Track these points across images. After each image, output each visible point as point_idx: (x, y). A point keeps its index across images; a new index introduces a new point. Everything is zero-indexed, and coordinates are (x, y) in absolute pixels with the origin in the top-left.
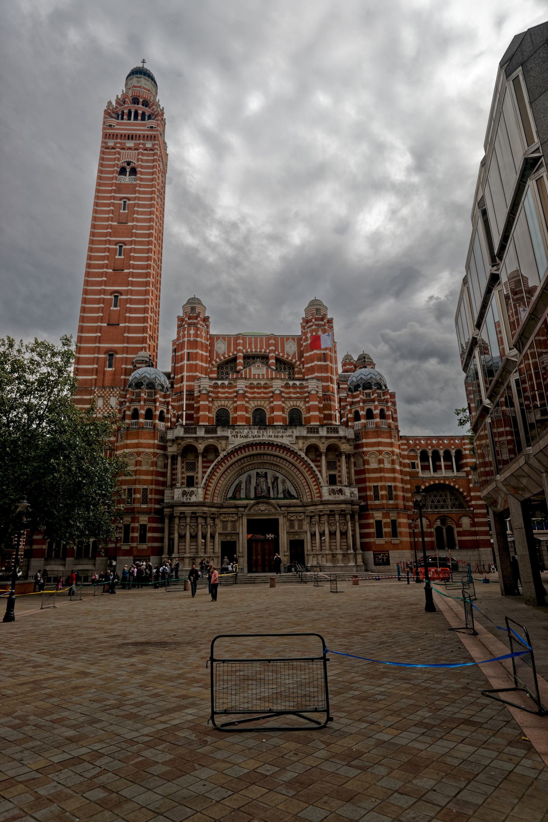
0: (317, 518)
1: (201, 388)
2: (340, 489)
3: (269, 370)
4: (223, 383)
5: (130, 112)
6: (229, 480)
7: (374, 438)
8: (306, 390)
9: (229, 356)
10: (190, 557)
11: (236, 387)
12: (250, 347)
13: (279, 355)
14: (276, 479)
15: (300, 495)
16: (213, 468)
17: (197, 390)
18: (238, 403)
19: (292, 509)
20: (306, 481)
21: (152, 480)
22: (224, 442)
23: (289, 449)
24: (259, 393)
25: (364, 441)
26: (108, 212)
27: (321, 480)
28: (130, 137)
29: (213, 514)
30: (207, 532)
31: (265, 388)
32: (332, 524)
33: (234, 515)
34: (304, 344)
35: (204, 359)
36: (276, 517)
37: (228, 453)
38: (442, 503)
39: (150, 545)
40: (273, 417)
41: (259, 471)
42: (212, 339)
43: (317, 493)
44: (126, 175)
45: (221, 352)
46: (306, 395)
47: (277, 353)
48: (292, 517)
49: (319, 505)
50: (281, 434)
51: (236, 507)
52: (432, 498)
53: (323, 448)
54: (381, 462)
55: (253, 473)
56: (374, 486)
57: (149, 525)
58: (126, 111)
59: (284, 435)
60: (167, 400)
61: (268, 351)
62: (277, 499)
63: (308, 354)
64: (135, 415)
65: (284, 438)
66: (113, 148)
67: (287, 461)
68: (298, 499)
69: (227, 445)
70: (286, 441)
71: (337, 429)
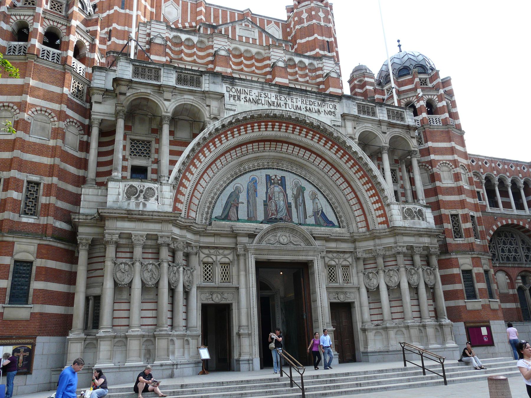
0: (380, 261)
1: (152, 37)
2: (420, 211)
3: (264, 35)
4: (188, 40)
6: (216, 184)
7: (444, 141)
8: (320, 72)
10: (143, 336)
11: (212, 47)
14: (301, 190)
15: (342, 222)
16: (193, 150)
17: (144, 40)
19: (332, 245)
21: (52, 167)
22: (214, 104)
23: (331, 134)
24: (247, 66)
25: (430, 144)
27: (386, 193)
29: (188, 245)
30: (177, 281)
31: (258, 61)
32: (413, 271)
33: (227, 252)
34: (298, 27)
36: (310, 258)
37: (223, 126)
38: (514, 254)
39: (38, 308)
41: (271, 173)
43: (379, 216)
46: (321, 79)
48: (332, 259)
49: (386, 236)
50: (316, 108)
51: (234, 235)
52: (502, 245)
53: (384, 140)
54: (457, 177)
55: (261, 175)
56: (452, 215)
57: (39, 263)
59: (322, 109)
60: (91, 29)
62: (305, 224)
63: (303, 41)
65: (322, 114)
68: (340, 227)
70: (326, 119)
71: (401, 115)
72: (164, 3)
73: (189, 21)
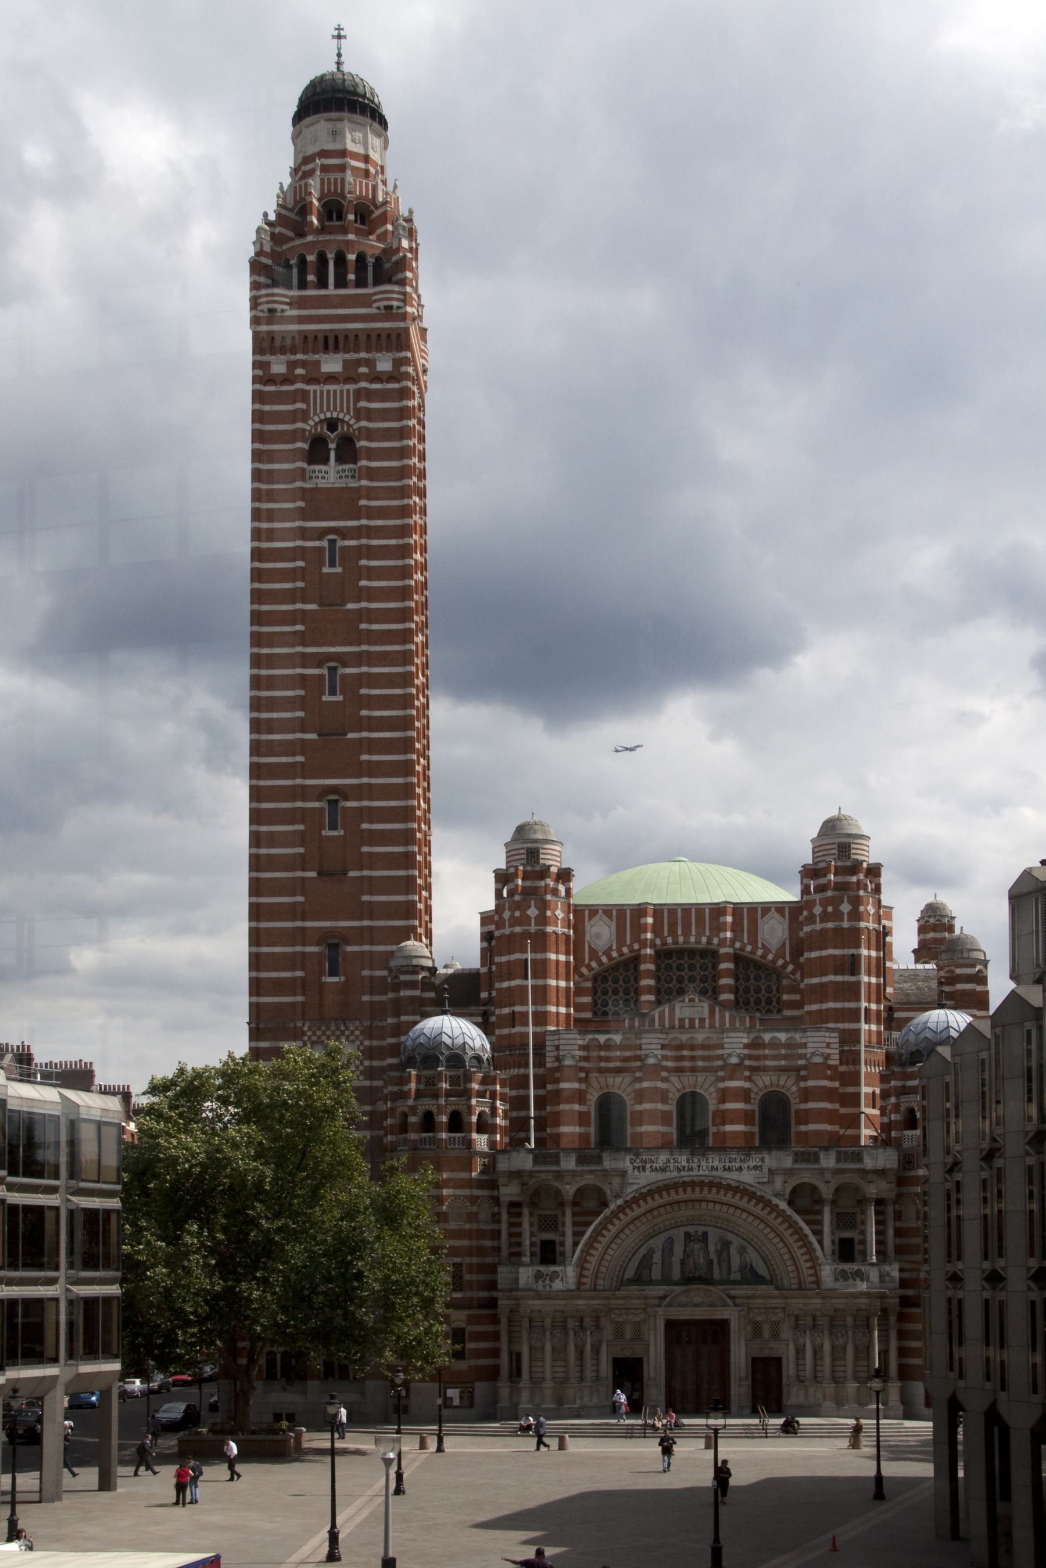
9: (623, 954)
12: (673, 932)
13: (742, 949)
17: (552, 1054)
18: (645, 1084)
20: (790, 1252)
35: (562, 970)
37: (626, 1202)
40: (724, 1112)
42: (581, 915)
45: (601, 944)
47: (738, 945)
61: (715, 941)
64: (428, 1122)
67: (750, 1214)
69: (623, 1185)
72: (590, 919)
73: (628, 943)
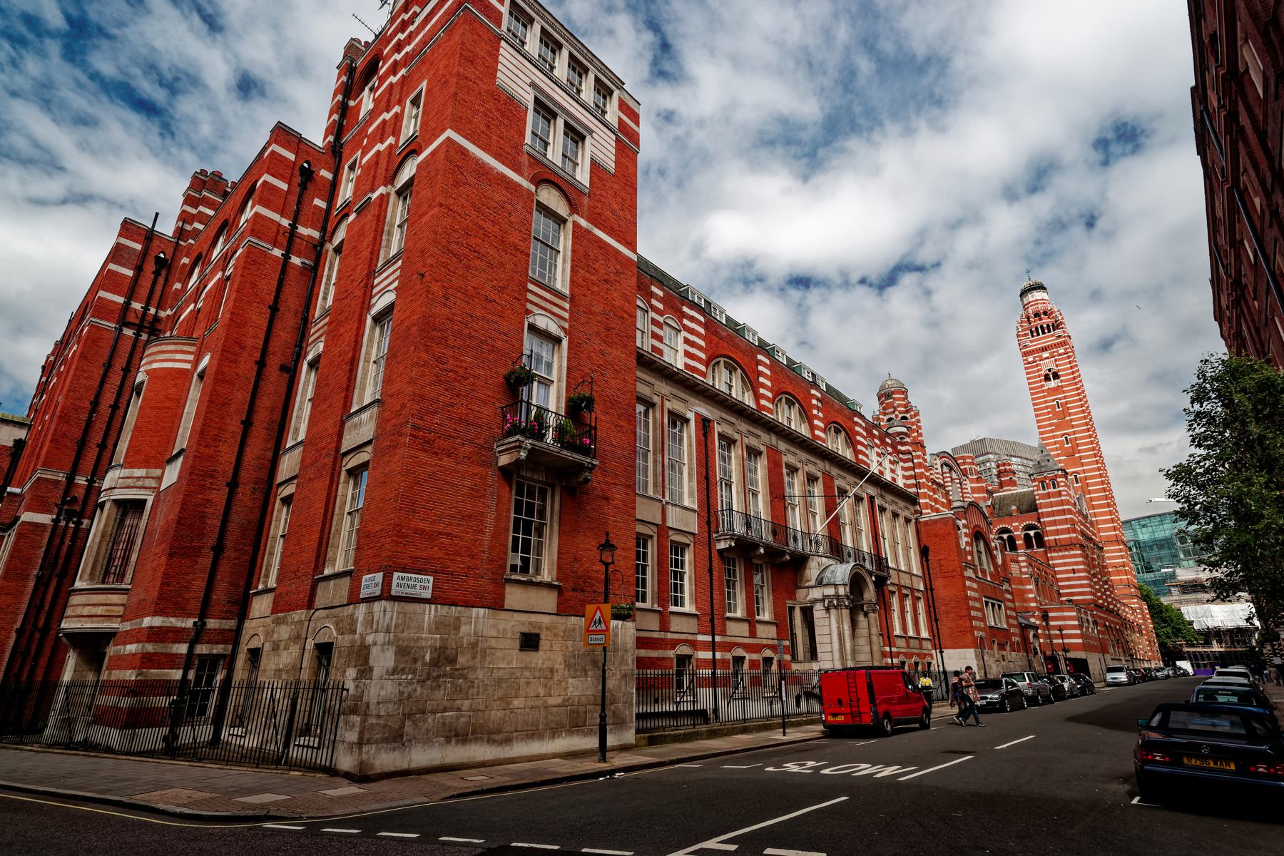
5: (1037, 328)
26: (1048, 413)
28: (1044, 349)
44: (1050, 380)
58: (1033, 329)
66: (1034, 362)
